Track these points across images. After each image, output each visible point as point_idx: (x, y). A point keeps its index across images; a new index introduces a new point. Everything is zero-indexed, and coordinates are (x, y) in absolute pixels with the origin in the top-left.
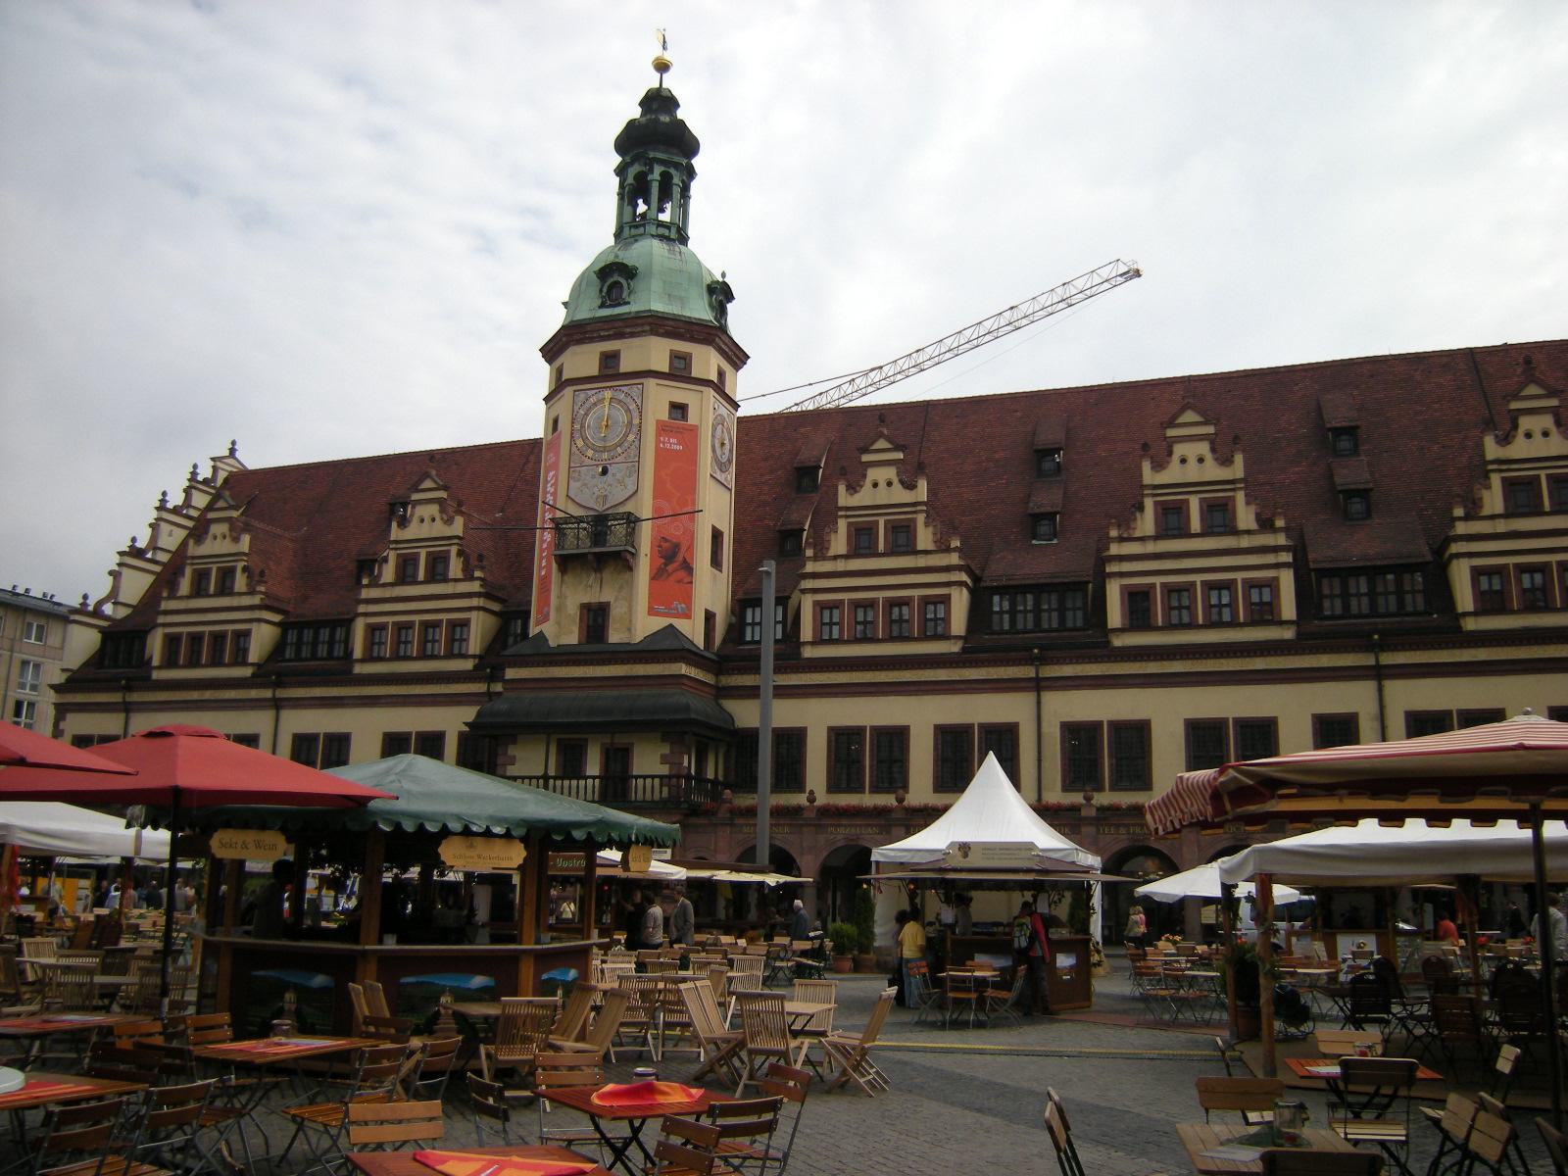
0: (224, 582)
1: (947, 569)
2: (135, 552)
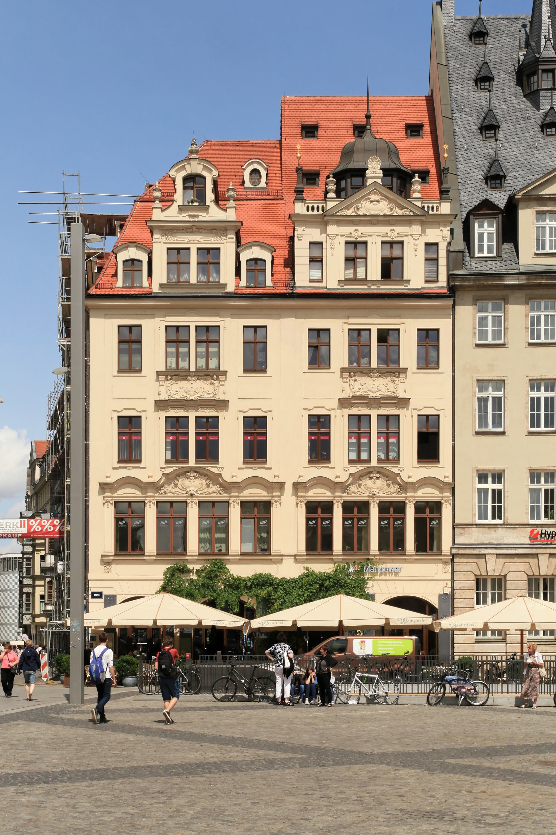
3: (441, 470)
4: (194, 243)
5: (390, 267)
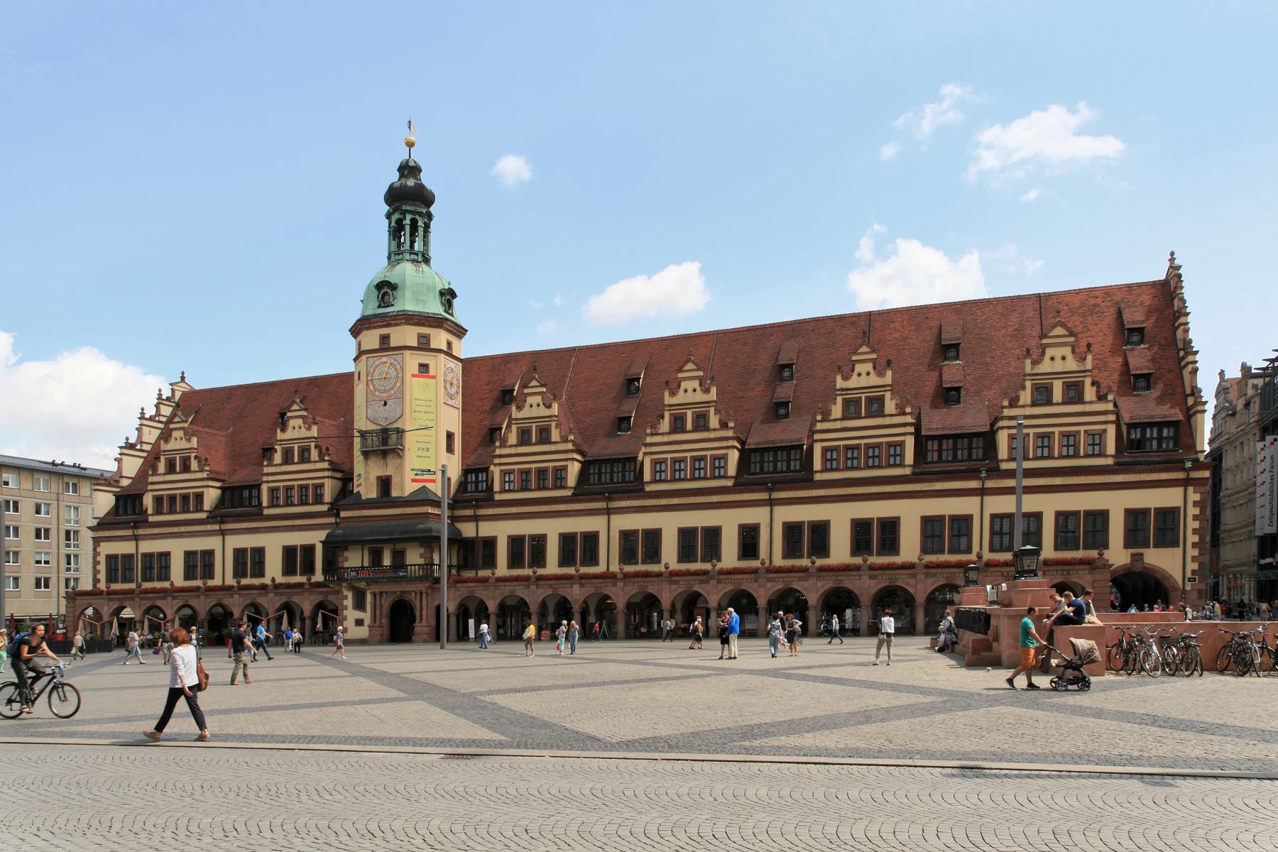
1: (566, 452)
2: (131, 446)
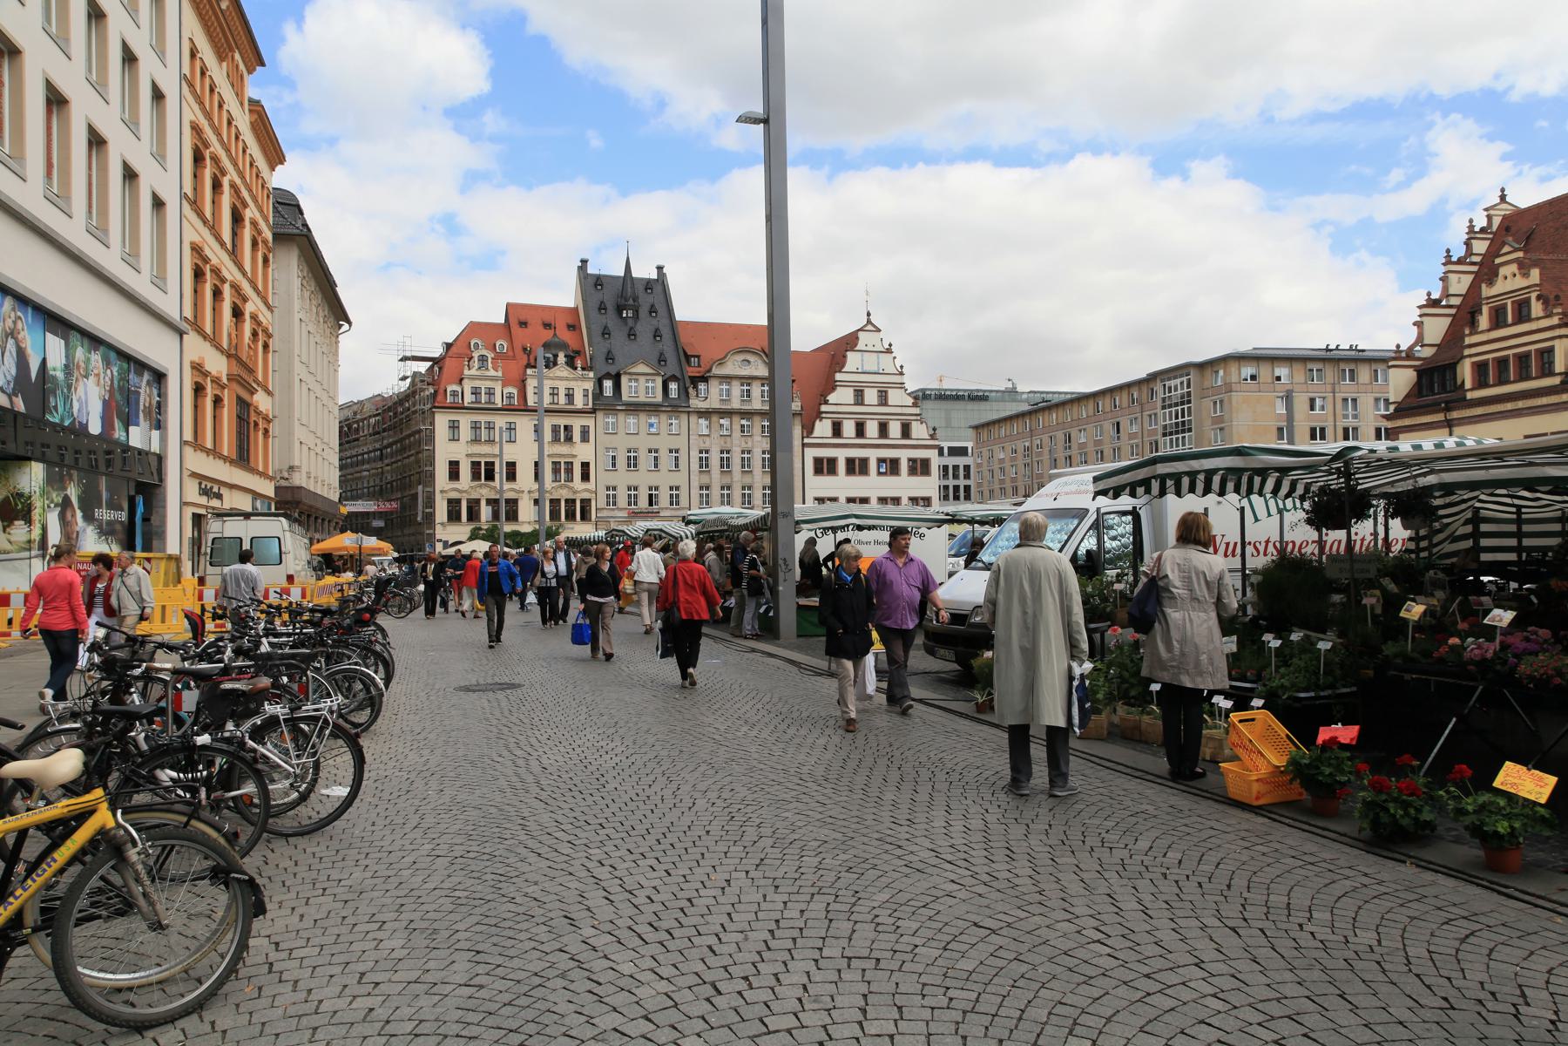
0: (1520, 312)
2: (1434, 303)
3: (591, 485)
4: (483, 385)
5: (570, 396)
